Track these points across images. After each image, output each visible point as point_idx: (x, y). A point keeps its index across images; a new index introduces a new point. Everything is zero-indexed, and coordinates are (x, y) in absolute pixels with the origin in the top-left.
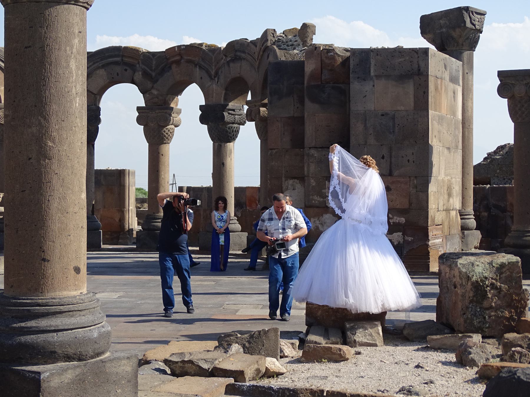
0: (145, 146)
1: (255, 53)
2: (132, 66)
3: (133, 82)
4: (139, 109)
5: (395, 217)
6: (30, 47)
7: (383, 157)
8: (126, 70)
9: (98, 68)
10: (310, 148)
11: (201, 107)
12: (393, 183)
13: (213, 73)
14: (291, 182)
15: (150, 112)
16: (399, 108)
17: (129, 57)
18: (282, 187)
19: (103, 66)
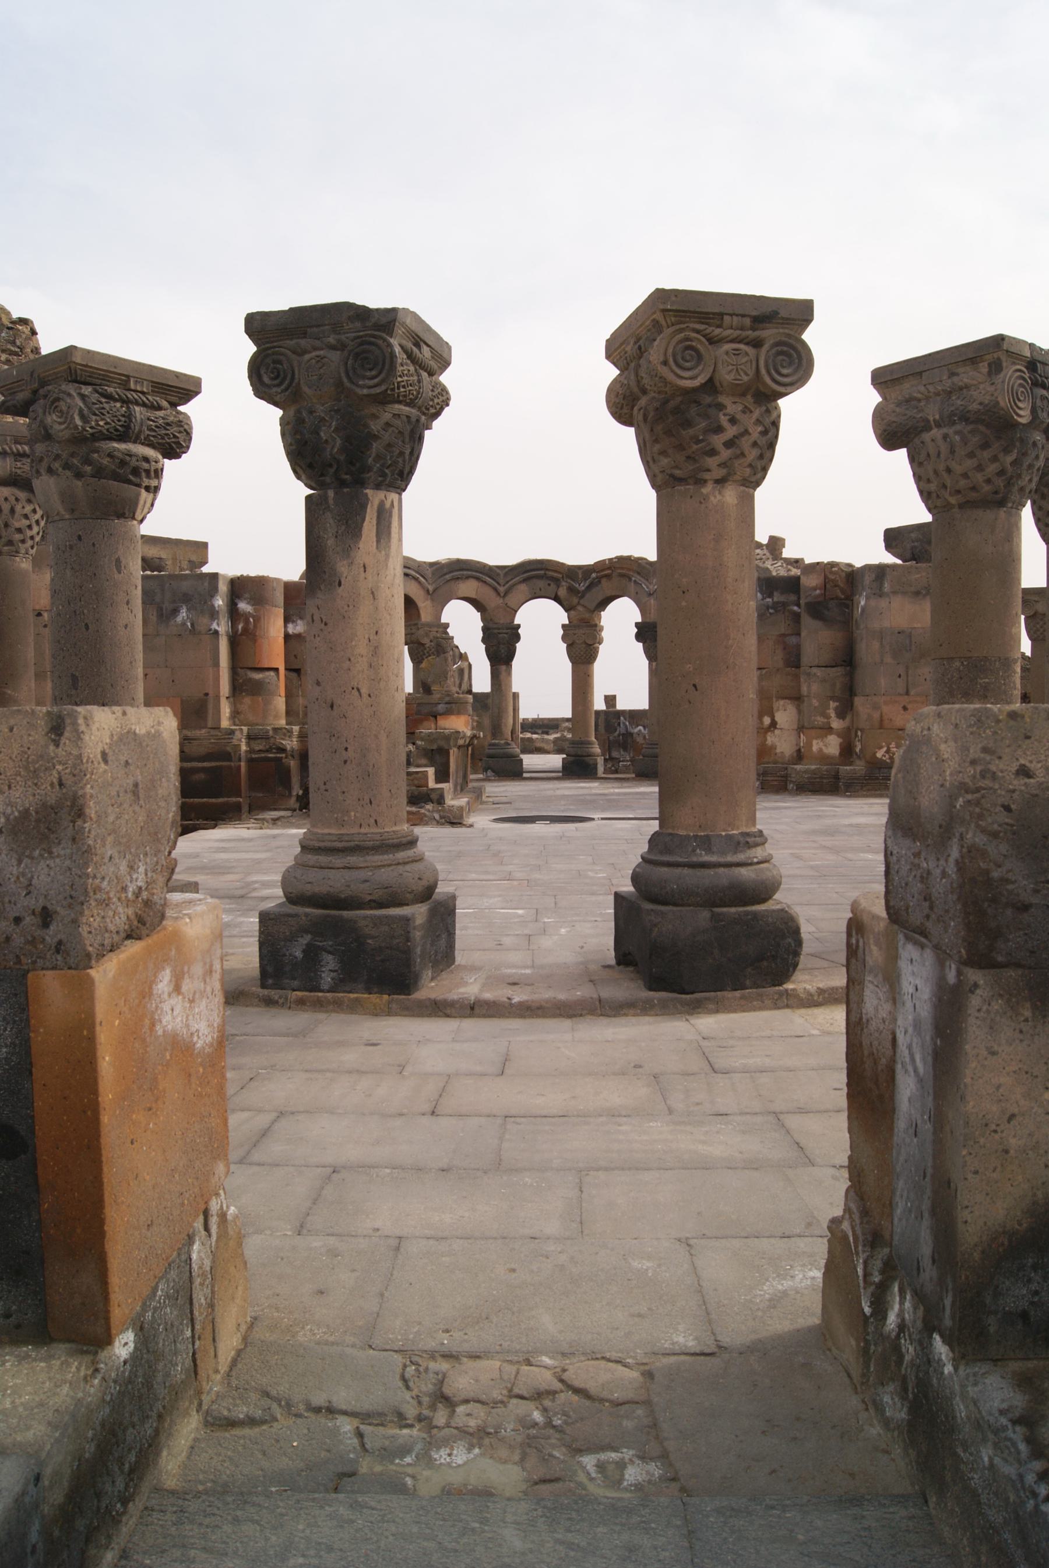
2: (557, 581)
3: (557, 599)
4: (564, 626)
7: (900, 676)
8: (549, 585)
9: (520, 582)
11: (637, 625)
12: (910, 702)
14: (782, 702)
16: (916, 626)
18: (772, 708)
19: (525, 580)
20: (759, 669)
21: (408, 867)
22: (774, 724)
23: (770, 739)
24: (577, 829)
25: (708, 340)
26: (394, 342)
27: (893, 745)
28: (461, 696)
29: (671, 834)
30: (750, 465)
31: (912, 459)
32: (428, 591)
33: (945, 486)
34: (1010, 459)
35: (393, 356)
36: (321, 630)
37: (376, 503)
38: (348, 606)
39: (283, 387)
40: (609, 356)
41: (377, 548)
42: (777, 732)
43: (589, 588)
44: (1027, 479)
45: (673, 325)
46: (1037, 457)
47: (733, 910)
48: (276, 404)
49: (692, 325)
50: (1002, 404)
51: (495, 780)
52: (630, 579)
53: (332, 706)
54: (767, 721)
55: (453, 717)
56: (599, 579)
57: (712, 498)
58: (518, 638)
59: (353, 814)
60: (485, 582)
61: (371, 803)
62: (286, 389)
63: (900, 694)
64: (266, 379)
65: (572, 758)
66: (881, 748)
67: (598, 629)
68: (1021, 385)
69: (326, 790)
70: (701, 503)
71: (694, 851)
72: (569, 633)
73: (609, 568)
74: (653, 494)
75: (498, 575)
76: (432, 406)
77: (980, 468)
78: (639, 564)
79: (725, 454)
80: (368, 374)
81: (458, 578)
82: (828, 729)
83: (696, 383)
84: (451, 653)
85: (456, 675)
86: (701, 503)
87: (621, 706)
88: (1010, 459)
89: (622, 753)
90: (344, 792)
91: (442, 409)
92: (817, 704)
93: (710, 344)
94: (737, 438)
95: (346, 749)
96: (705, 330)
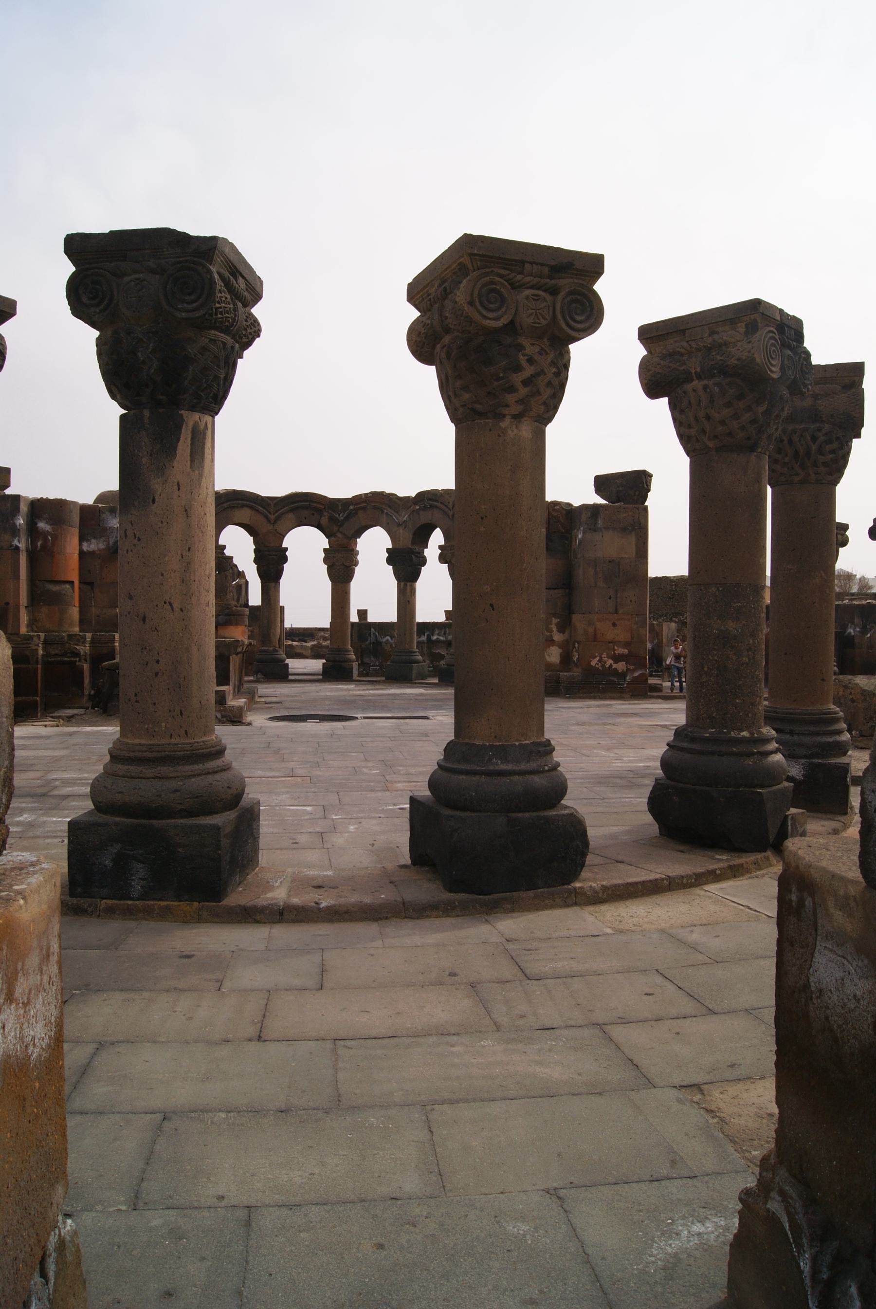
1: (449, 502)
2: (320, 512)
3: (319, 527)
4: (325, 550)
5: (620, 649)
6: (815, 517)
7: (610, 598)
8: (313, 514)
9: (287, 512)
11: (388, 550)
17: (316, 502)
19: (292, 510)
21: (217, 777)
24: (344, 728)
25: (511, 284)
26: (214, 269)
27: (604, 655)
28: (239, 609)
29: (468, 744)
30: (545, 403)
31: (673, 406)
33: (704, 432)
34: (761, 409)
35: (212, 281)
36: (135, 545)
37: (191, 424)
38: (162, 522)
39: (101, 307)
40: (410, 299)
41: (191, 467)
43: (347, 518)
44: (775, 427)
45: (479, 269)
46: (783, 409)
47: (527, 815)
48: (93, 325)
49: (496, 270)
50: (758, 360)
51: (264, 682)
52: (383, 512)
53: (144, 620)
55: (232, 628)
56: (356, 511)
57: (510, 432)
58: (285, 559)
59: (163, 724)
60: (257, 510)
61: (181, 714)
62: (105, 309)
63: (611, 613)
64: (84, 299)
65: (331, 664)
66: (595, 657)
67: (354, 553)
68: (773, 345)
69: (137, 702)
70: (499, 436)
71: (490, 759)
72: (330, 557)
73: (366, 502)
74: (452, 428)
75: (269, 504)
76: (245, 335)
77: (736, 416)
78: (391, 500)
79: (523, 391)
80: (187, 298)
81: (234, 507)
83: (500, 323)
84: (231, 571)
85: (235, 591)
86: (499, 436)
87: (371, 618)
88: (761, 409)
89: (372, 659)
90: (155, 704)
91: (253, 340)
93: (513, 288)
94: (534, 377)
95: (158, 662)
96: (508, 275)
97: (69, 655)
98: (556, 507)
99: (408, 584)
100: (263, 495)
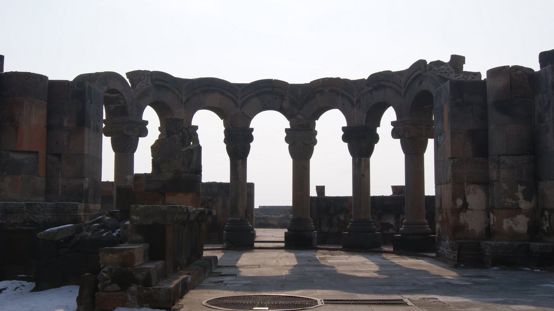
0: (288, 162)
1: (400, 82)
4: (287, 130)
8: (276, 98)
10: (499, 156)
11: (344, 129)
13: (355, 100)
14: (472, 187)
15: (297, 133)
20: (452, 158)
22: (465, 206)
23: (463, 218)
32: (182, 100)
42: (468, 212)
54: (460, 202)
58: (251, 139)
82: (517, 210)
92: (506, 188)
97: (28, 224)
98: (518, 72)
99: (363, 159)
100: (232, 82)
